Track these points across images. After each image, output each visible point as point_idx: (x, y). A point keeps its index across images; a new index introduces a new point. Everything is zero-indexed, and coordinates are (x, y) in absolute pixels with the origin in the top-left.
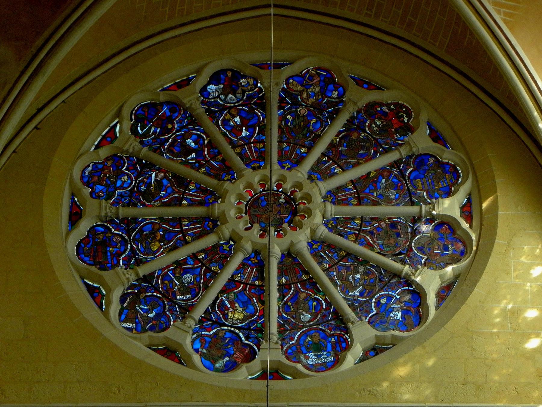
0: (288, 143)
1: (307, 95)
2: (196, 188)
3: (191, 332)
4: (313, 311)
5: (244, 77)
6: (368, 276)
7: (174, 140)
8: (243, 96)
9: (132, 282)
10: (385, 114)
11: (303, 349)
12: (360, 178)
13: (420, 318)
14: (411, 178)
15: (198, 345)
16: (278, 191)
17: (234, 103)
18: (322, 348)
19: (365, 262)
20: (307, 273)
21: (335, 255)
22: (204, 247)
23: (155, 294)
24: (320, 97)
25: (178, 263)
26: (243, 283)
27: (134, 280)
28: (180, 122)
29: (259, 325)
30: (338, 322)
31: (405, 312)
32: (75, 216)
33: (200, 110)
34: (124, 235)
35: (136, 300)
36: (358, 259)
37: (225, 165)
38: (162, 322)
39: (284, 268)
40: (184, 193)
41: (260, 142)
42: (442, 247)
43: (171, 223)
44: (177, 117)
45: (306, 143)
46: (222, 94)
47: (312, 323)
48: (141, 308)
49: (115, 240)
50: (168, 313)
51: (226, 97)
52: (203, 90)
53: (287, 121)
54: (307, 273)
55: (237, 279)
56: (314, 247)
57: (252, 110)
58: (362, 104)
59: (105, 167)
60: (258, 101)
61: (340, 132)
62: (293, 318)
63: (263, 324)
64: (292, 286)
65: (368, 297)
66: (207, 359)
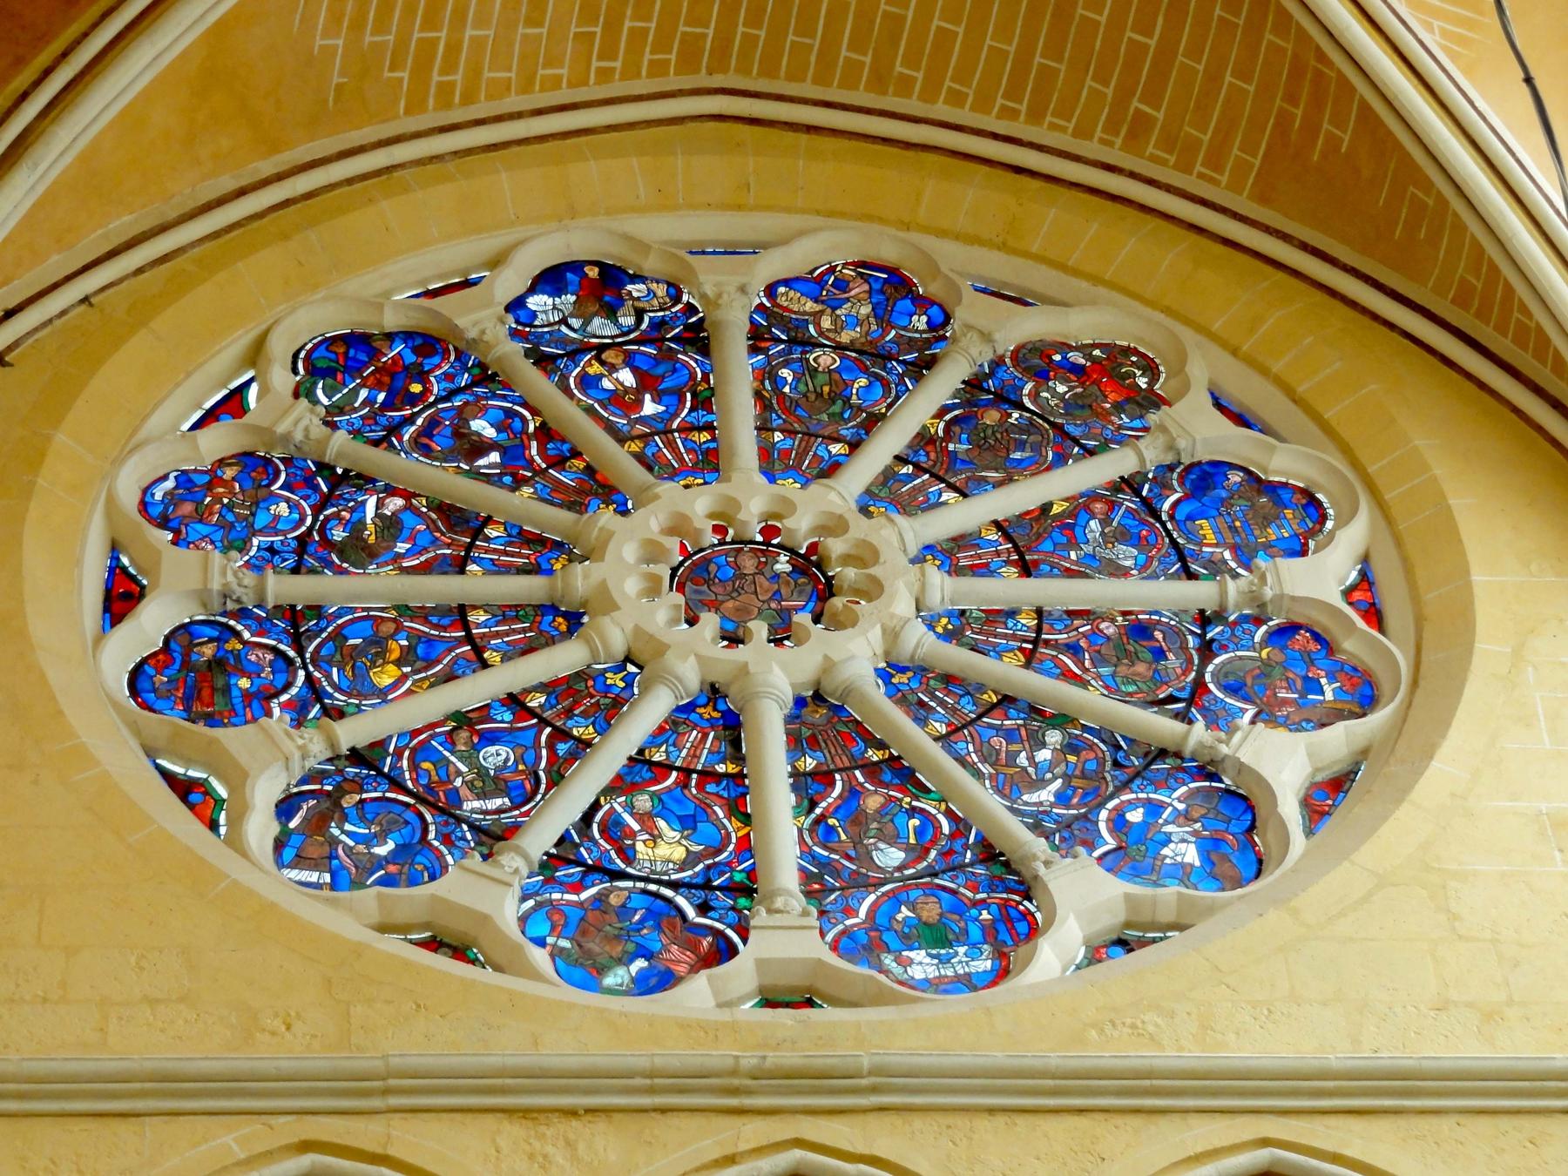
0: (789, 432)
1: (834, 322)
2: (509, 536)
3: (517, 893)
4: (912, 841)
5: (637, 278)
6: (1078, 756)
7: (433, 423)
8: (639, 321)
9: (311, 763)
10: (1077, 370)
11: (888, 937)
12: (1022, 516)
13: (1260, 862)
14: (1180, 516)
15: (541, 927)
16: (767, 543)
17: (612, 337)
18: (951, 937)
19: (1062, 720)
20: (881, 745)
21: (964, 701)
22: (545, 679)
23: (388, 795)
24: (874, 327)
25: (462, 719)
26: (678, 769)
27: (323, 758)
28: (449, 377)
29: (738, 877)
30: (998, 870)
31: (1211, 847)
32: (122, 596)
33: (509, 352)
34: (282, 647)
35: (330, 808)
36: (1041, 713)
37: (596, 481)
38: (419, 868)
39: (806, 732)
40: (469, 547)
41: (700, 429)
42: (1299, 683)
43: (434, 620)
44: (439, 366)
45: (844, 432)
46: (571, 315)
47: (912, 871)
48: (344, 833)
49: (253, 658)
50: (436, 843)
51: (587, 323)
52: (517, 305)
53: (777, 382)
54: (881, 745)
55: (656, 758)
56: (895, 681)
57: (670, 355)
58: (1007, 341)
59: (215, 480)
60: (687, 335)
61: (944, 410)
62: (848, 857)
63: (751, 873)
64: (838, 777)
65: (1085, 805)
66: (576, 963)
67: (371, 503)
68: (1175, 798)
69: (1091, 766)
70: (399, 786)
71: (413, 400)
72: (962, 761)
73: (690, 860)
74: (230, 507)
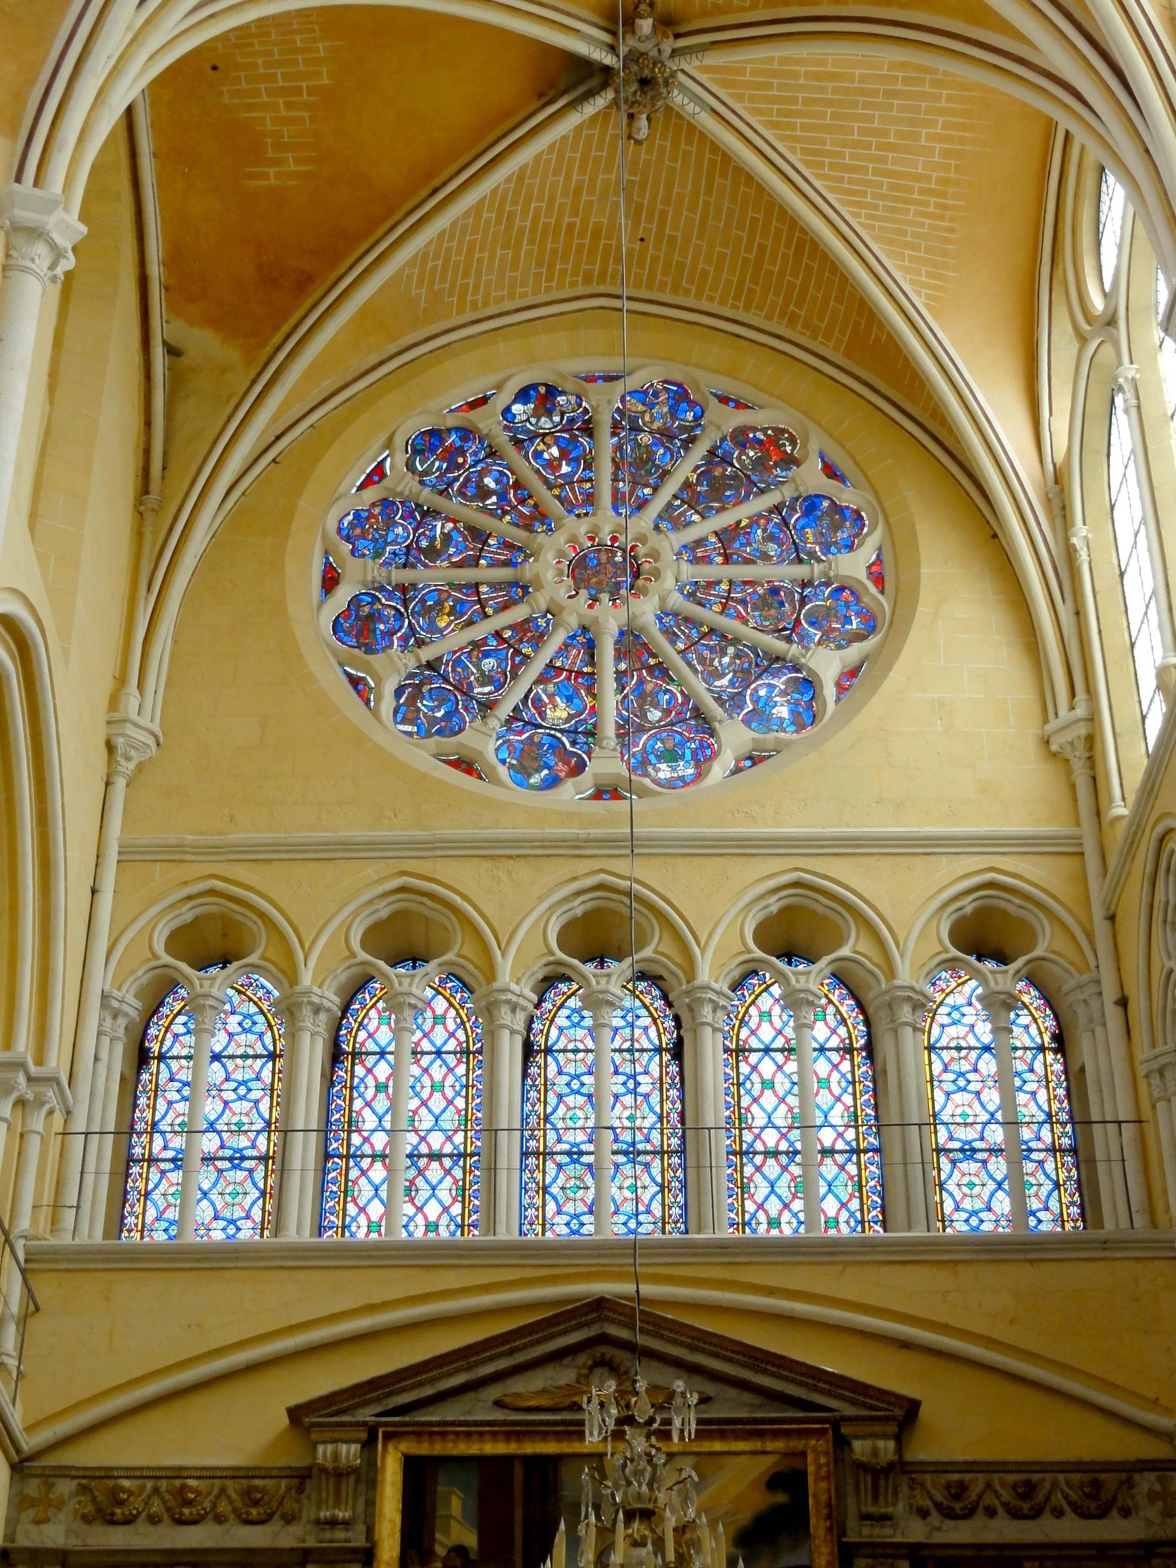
3: (495, 737)
5: (563, 393)
7: (467, 479)
10: (760, 442)
12: (726, 529)
15: (504, 754)
19: (736, 641)
20: (654, 656)
25: (476, 645)
28: (475, 454)
29: (589, 727)
30: (700, 722)
32: (330, 581)
33: (502, 438)
35: (417, 694)
39: (623, 650)
40: (482, 550)
41: (587, 481)
48: (424, 705)
52: (507, 411)
57: (574, 439)
61: (698, 467)
63: (595, 726)
67: (439, 525)
68: (780, 683)
69: (746, 665)
70: (447, 681)
71: (460, 466)
72: (689, 664)
73: (570, 718)
74: (377, 530)
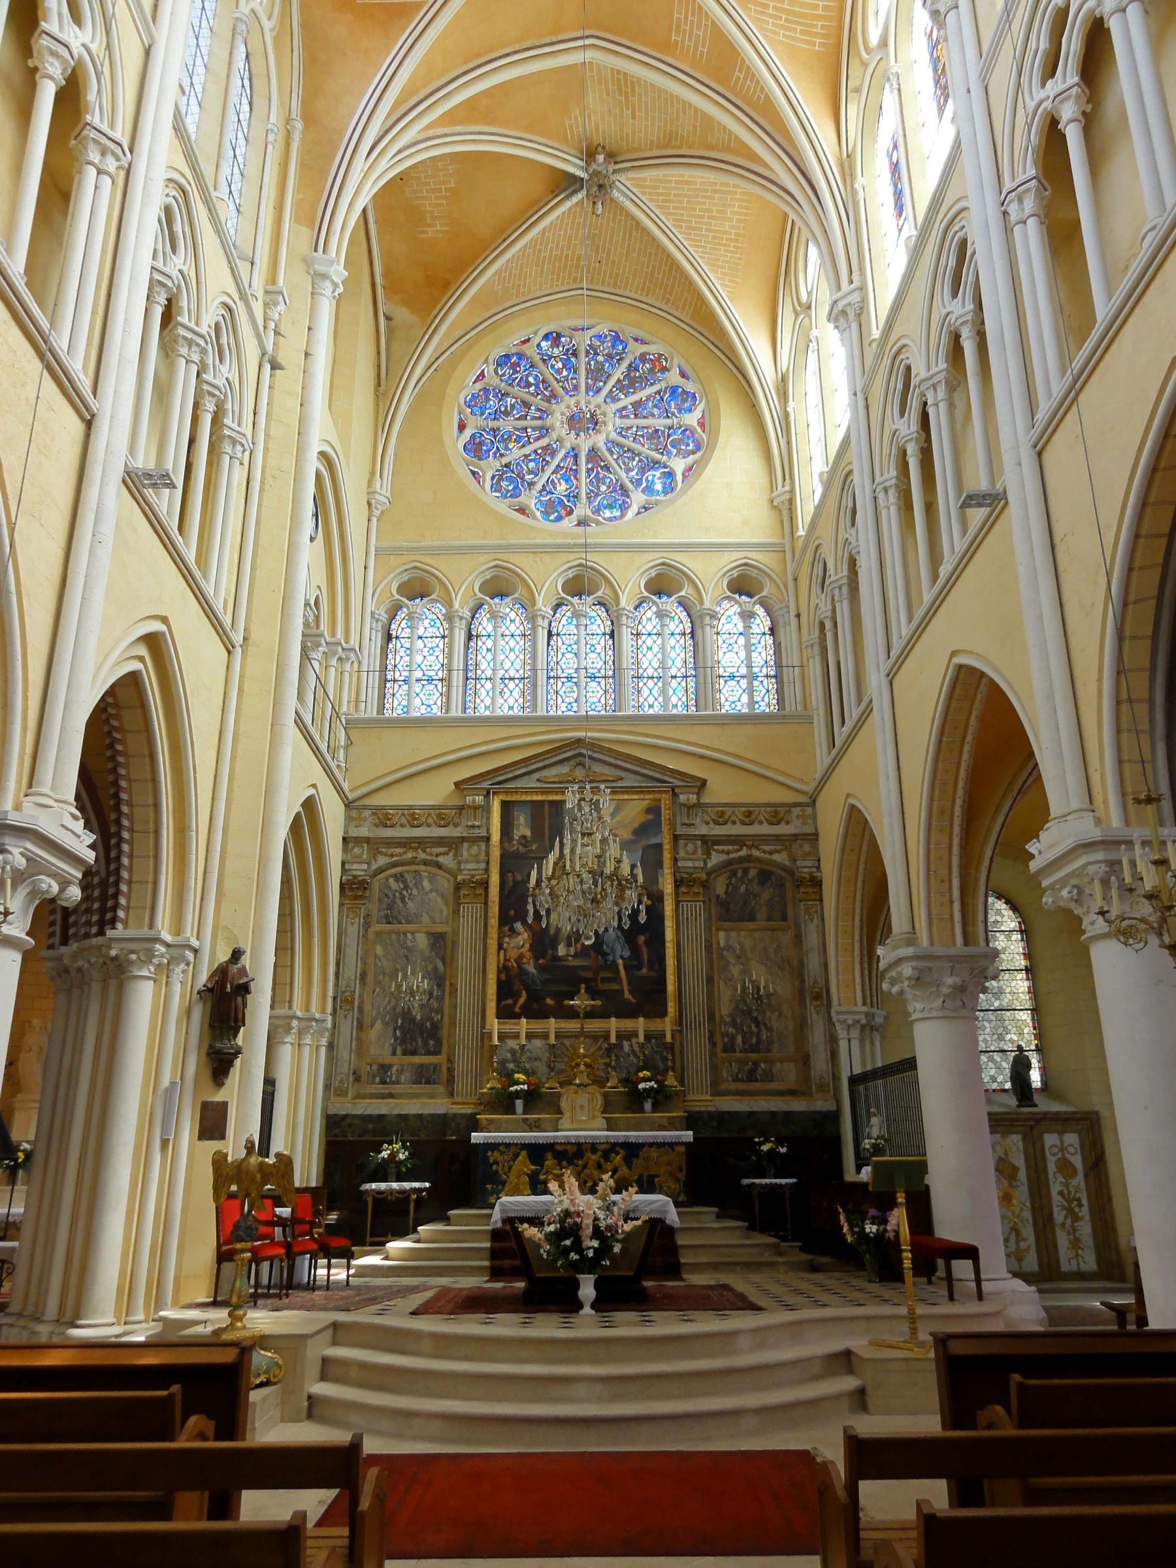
15: (539, 506)
19: (639, 454)
25: (526, 456)
32: (462, 427)
35: (501, 478)
57: (569, 359)
